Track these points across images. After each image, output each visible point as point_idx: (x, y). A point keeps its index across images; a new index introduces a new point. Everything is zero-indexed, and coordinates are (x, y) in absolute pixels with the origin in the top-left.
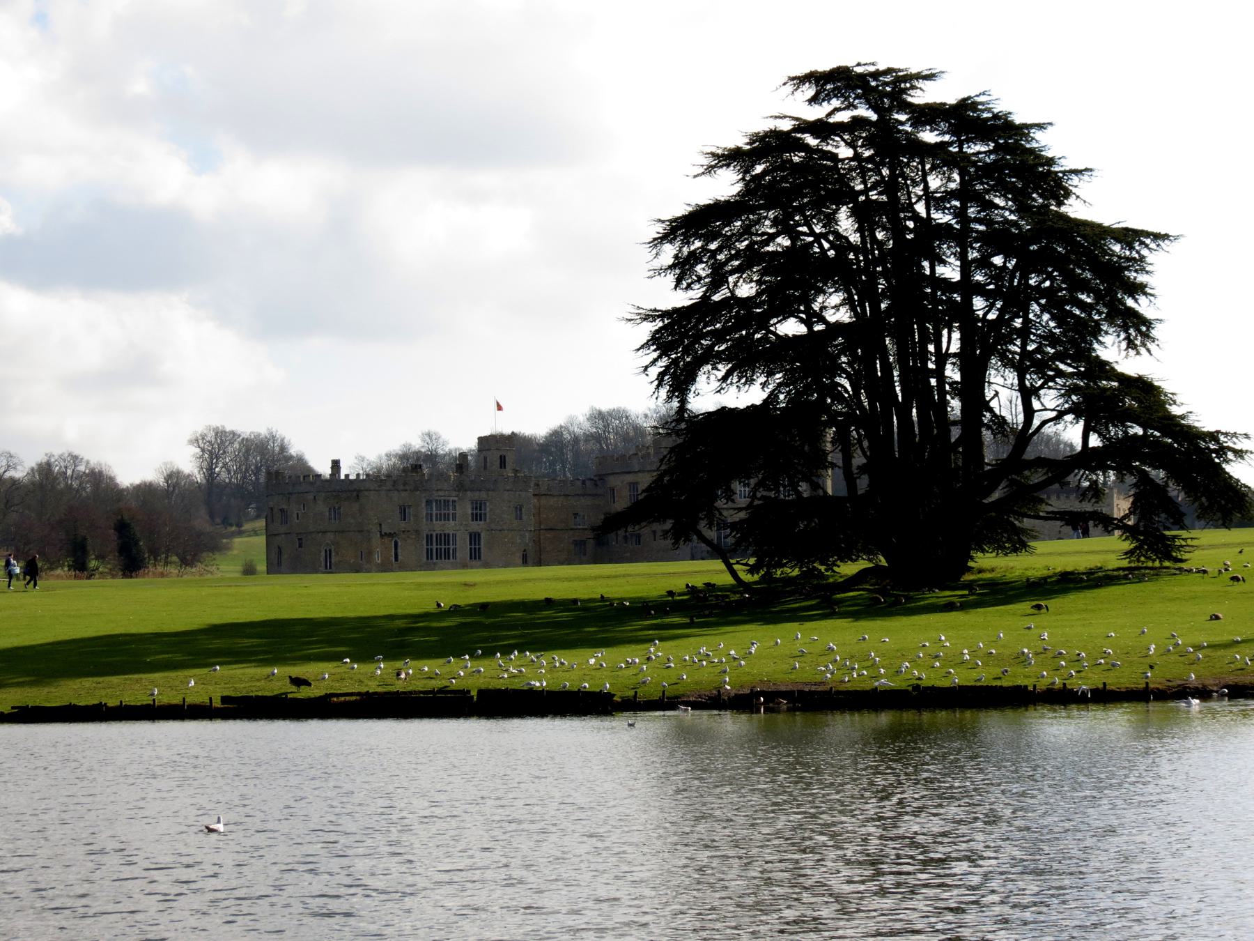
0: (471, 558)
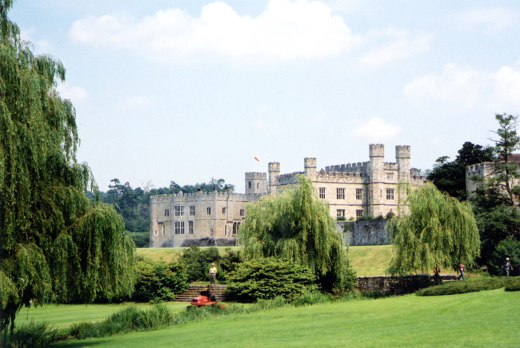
0: (190, 233)
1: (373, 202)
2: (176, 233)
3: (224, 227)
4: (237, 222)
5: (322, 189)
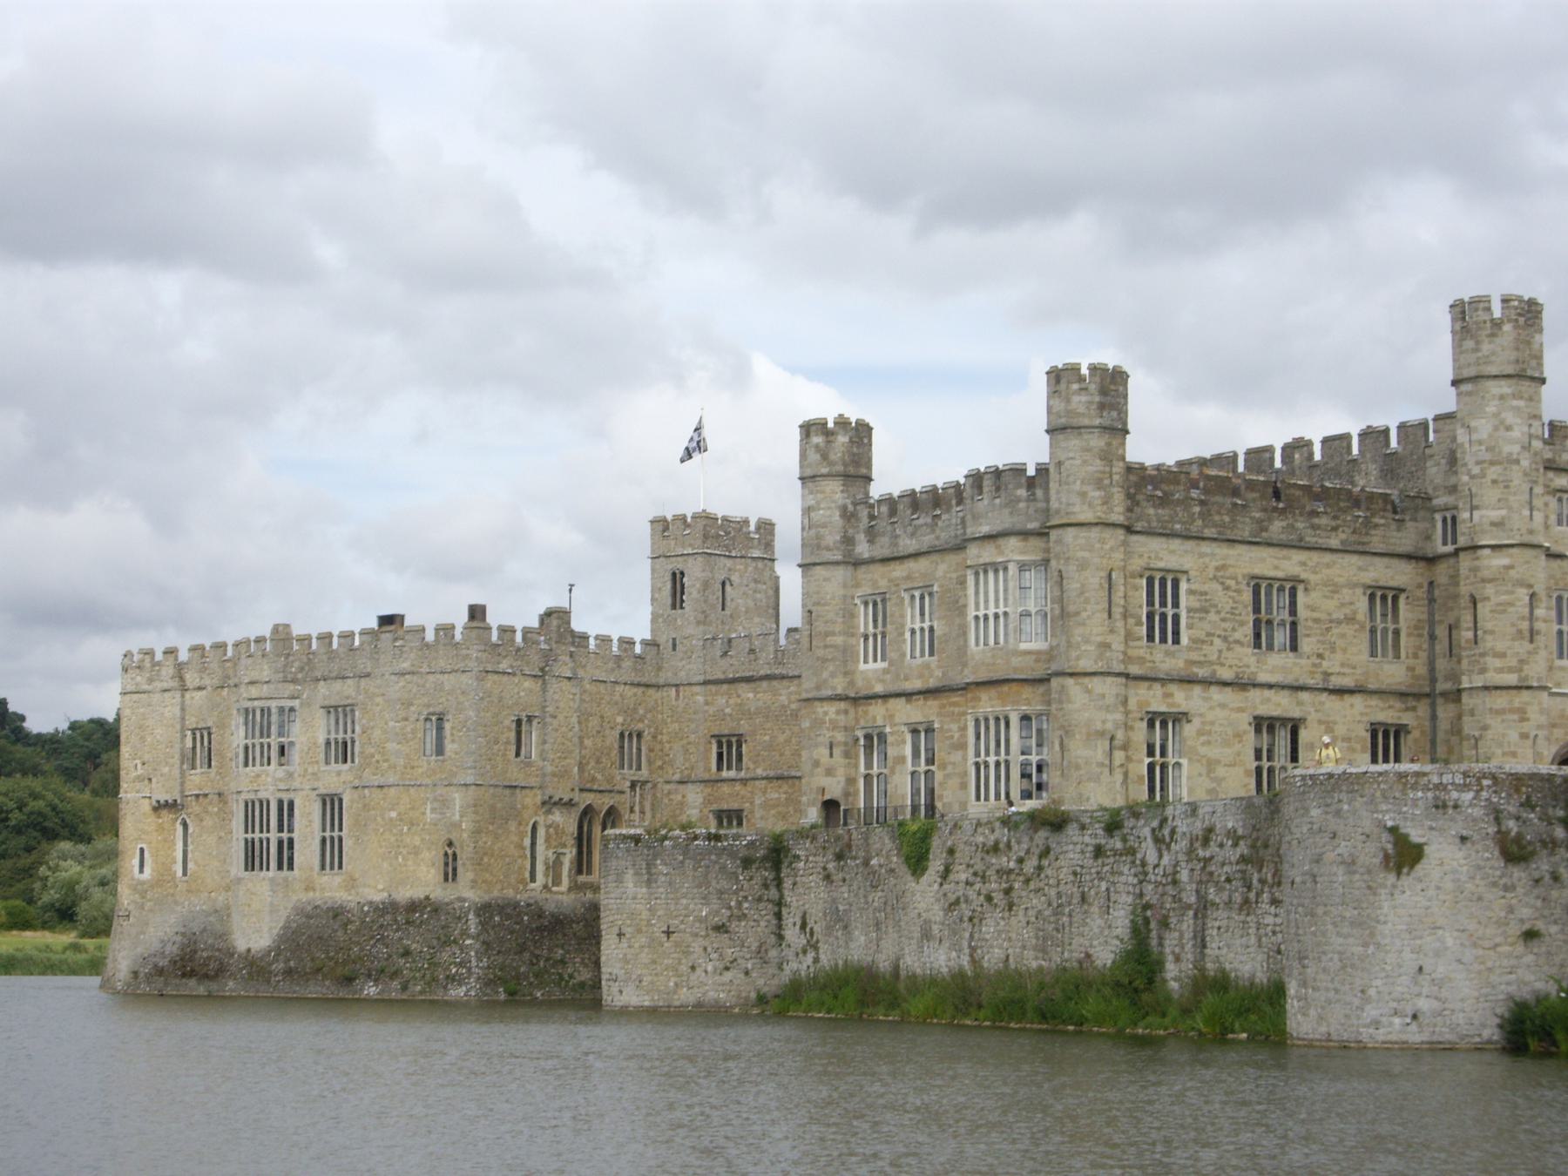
0: (323, 867)
1: (1483, 671)
2: (250, 864)
3: (522, 835)
4: (603, 803)
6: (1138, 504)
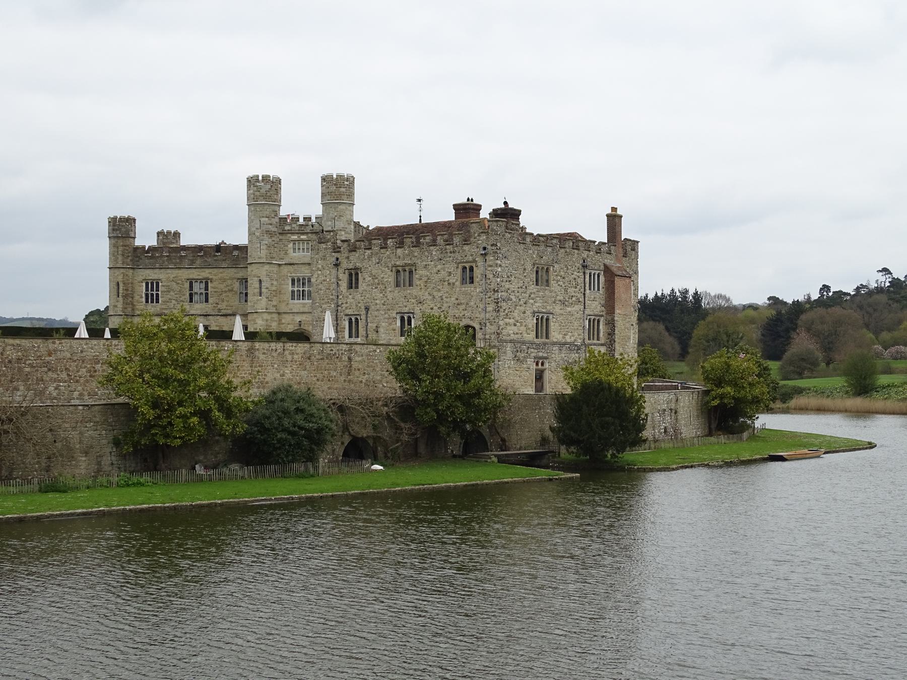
5: (152, 284)
6: (141, 259)
